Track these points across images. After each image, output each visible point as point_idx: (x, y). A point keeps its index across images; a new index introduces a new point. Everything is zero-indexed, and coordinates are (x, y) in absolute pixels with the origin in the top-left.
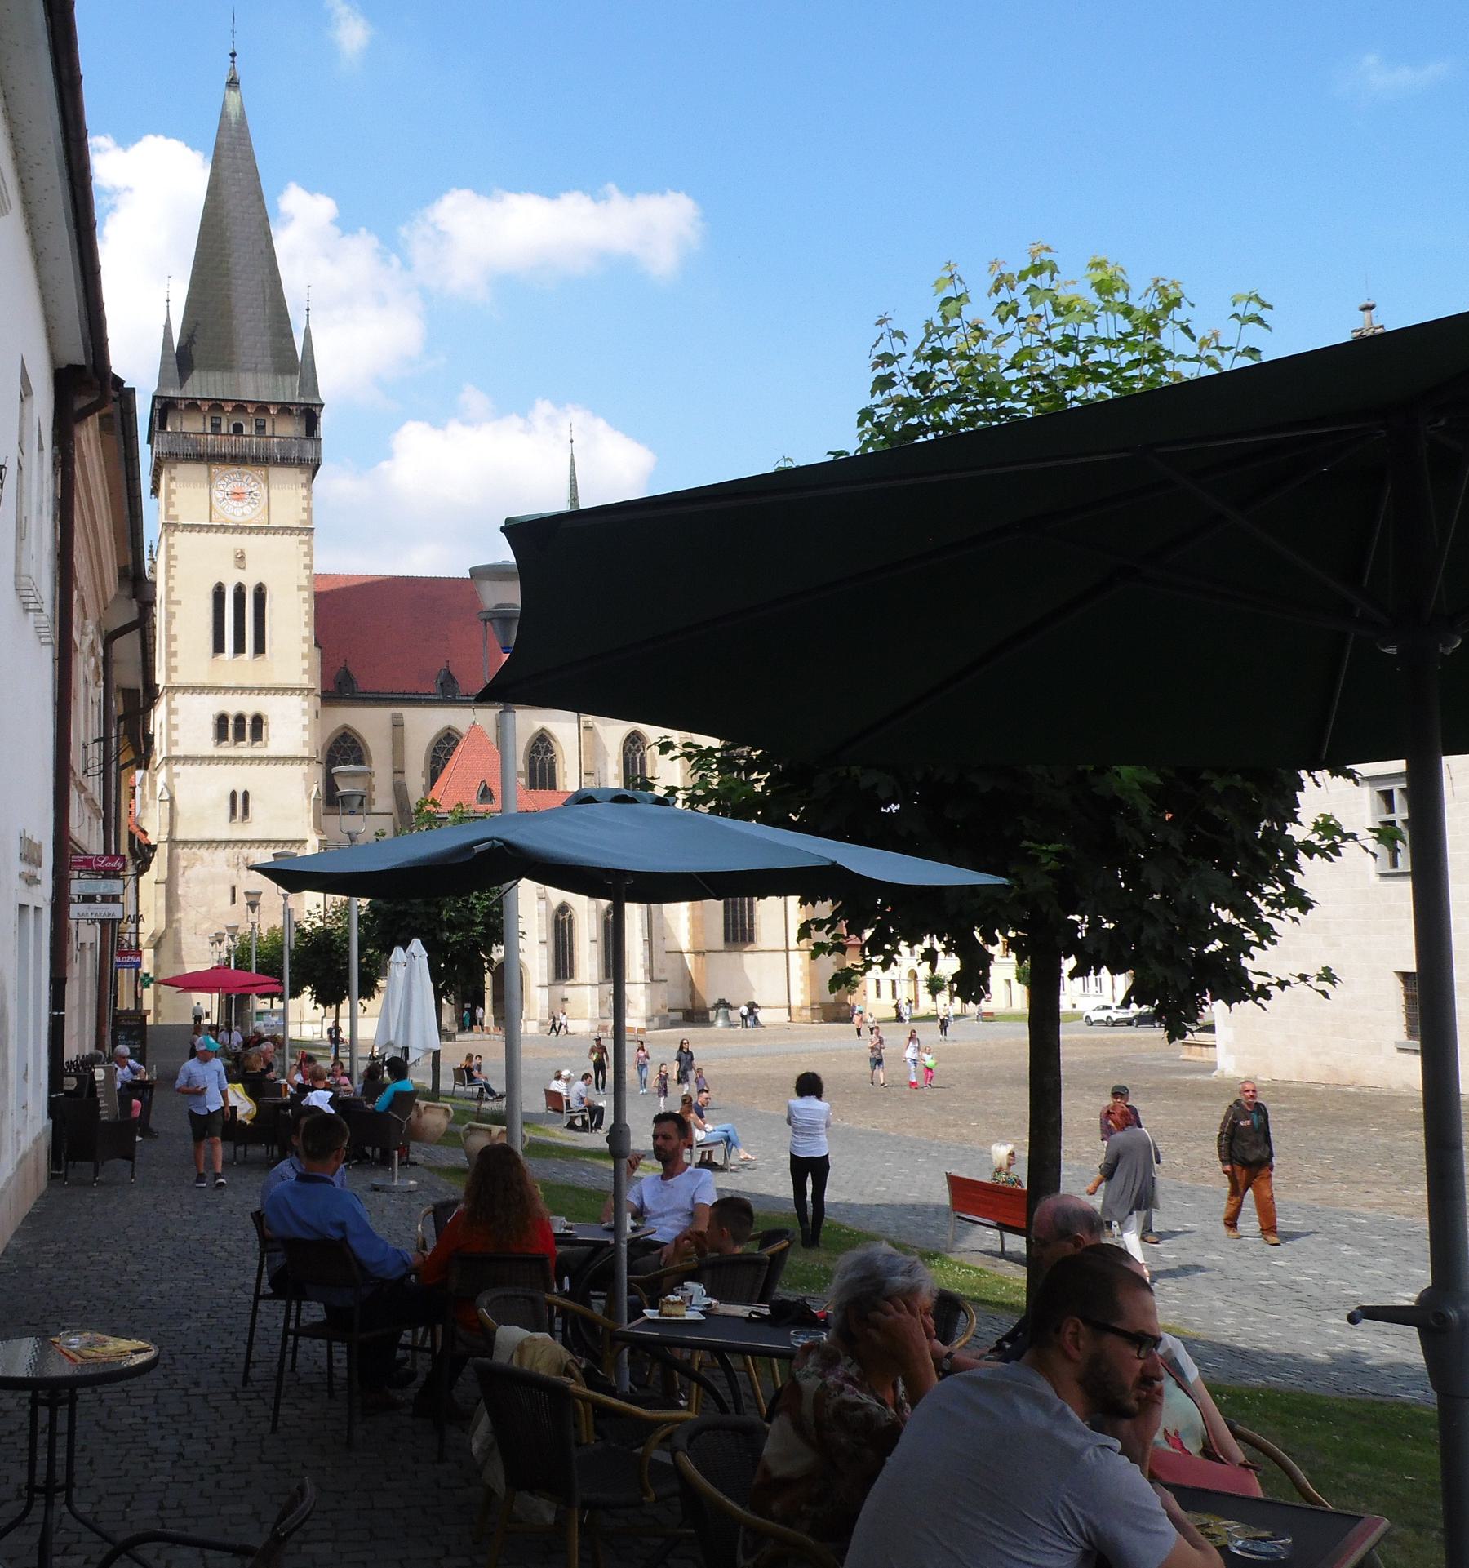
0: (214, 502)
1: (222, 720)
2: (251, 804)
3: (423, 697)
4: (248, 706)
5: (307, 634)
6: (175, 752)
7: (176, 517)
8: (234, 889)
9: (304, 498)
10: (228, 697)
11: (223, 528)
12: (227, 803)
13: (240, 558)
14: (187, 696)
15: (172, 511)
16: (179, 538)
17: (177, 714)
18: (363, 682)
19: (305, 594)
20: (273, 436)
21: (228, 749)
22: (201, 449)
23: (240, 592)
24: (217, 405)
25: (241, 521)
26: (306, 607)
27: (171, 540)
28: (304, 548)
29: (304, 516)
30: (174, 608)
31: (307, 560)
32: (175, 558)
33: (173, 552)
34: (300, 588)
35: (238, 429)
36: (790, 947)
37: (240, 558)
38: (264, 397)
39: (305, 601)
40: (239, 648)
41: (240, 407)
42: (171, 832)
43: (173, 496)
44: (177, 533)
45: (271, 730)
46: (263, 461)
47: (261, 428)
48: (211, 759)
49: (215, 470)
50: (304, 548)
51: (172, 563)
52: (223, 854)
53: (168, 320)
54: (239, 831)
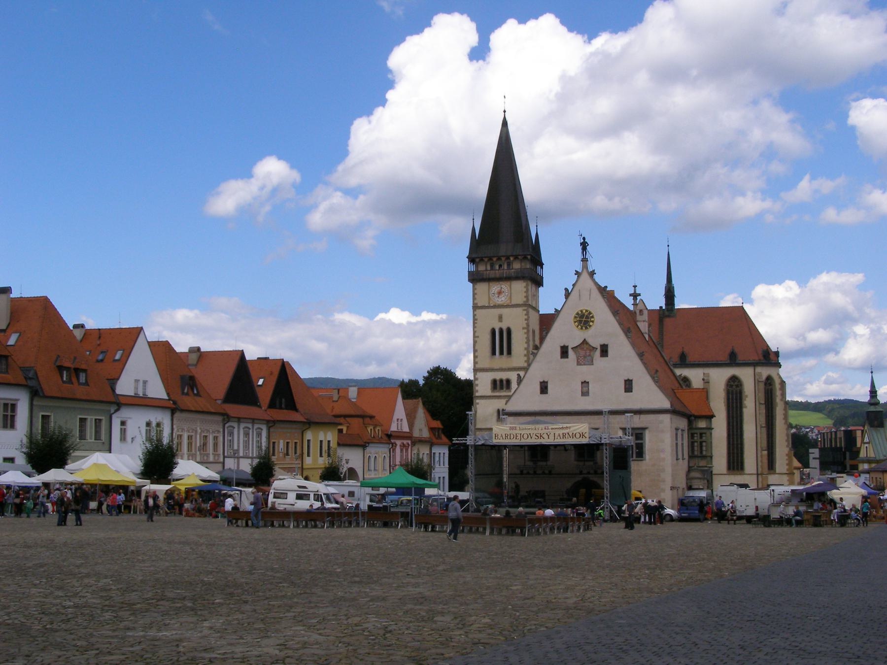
1: (494, 382)
4: (503, 376)
6: (477, 394)
7: (477, 304)
9: (525, 292)
11: (495, 307)
12: (496, 414)
13: (500, 318)
14: (481, 373)
15: (475, 302)
16: (478, 312)
19: (525, 331)
20: (512, 269)
22: (485, 277)
23: (501, 331)
27: (475, 313)
28: (525, 312)
29: (525, 299)
31: (526, 317)
32: (476, 320)
33: (476, 317)
34: (524, 328)
36: (759, 472)
37: (500, 318)
39: (525, 333)
46: (508, 279)
47: (509, 265)
49: (491, 284)
50: (525, 312)
53: (473, 227)
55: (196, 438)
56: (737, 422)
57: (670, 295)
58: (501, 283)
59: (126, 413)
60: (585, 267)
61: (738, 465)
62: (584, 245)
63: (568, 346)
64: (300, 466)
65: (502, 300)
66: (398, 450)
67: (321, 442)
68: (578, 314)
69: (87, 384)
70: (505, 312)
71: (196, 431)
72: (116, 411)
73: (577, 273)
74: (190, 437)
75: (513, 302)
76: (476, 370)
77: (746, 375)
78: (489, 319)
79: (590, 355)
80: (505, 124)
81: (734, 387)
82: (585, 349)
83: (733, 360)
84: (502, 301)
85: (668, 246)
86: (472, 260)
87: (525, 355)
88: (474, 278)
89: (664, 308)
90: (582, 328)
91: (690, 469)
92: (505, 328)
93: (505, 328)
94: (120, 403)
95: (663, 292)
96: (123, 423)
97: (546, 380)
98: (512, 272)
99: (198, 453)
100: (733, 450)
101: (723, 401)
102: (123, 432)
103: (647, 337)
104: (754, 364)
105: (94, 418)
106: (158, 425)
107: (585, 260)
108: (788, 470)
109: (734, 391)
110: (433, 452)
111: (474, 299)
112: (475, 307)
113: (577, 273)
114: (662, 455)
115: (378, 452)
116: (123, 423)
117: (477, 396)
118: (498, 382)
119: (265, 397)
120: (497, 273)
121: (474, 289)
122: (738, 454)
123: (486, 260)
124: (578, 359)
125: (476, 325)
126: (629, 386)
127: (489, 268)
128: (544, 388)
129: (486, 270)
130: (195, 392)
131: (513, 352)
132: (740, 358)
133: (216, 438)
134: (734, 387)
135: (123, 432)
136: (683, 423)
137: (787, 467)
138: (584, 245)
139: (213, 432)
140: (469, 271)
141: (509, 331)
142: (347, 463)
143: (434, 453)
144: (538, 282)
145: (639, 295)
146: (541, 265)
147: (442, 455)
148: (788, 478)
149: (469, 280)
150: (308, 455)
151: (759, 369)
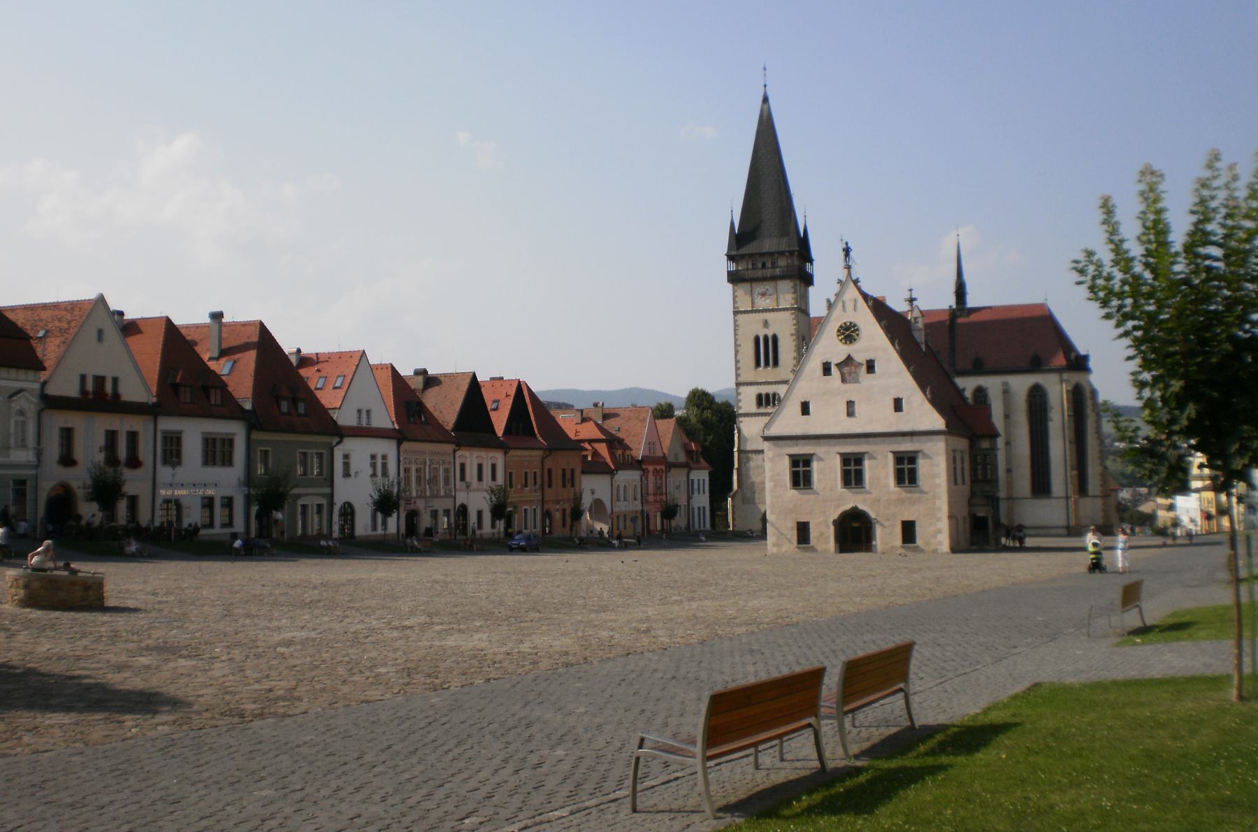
1: (759, 397)
6: (740, 412)
7: (738, 308)
10: (763, 386)
11: (759, 311)
13: (766, 324)
15: (736, 305)
16: (740, 317)
19: (794, 337)
20: (777, 267)
21: (762, 410)
22: (746, 277)
23: (766, 338)
24: (751, 256)
28: (793, 316)
30: (739, 348)
32: (738, 326)
33: (737, 323)
34: (792, 335)
35: (764, 265)
37: (766, 324)
38: (773, 250)
41: (762, 255)
42: (739, 448)
46: (774, 278)
47: (773, 263)
50: (793, 316)
55: (425, 468)
58: (765, 283)
59: (350, 445)
60: (849, 274)
62: (847, 251)
63: (830, 363)
64: (540, 498)
66: (651, 477)
67: (564, 470)
68: (841, 327)
69: (306, 415)
70: (770, 316)
71: (425, 463)
72: (338, 443)
73: (840, 282)
74: (418, 470)
76: (738, 384)
78: (754, 326)
80: (766, 100)
83: (1036, 365)
86: (731, 258)
88: (734, 278)
89: (954, 307)
90: (846, 343)
91: (973, 494)
92: (770, 335)
93: (770, 335)
94: (342, 433)
96: (346, 457)
97: (807, 400)
98: (778, 271)
99: (427, 486)
102: (347, 466)
103: (923, 347)
105: (315, 451)
106: (384, 457)
107: (848, 267)
110: (691, 478)
111: (735, 302)
112: (736, 313)
113: (840, 282)
114: (937, 481)
115: (630, 478)
116: (346, 457)
119: (499, 421)
120: (759, 273)
121: (734, 291)
125: (737, 332)
126: (898, 405)
127: (750, 266)
128: (805, 409)
129: (748, 269)
130: (423, 419)
133: (447, 470)
135: (347, 466)
136: (962, 444)
138: (847, 251)
139: (444, 463)
140: (728, 271)
141: (775, 338)
142: (593, 493)
143: (693, 480)
144: (808, 280)
145: (915, 299)
146: (811, 261)
147: (701, 482)
149: (729, 281)
150: (550, 486)
151: (1065, 376)
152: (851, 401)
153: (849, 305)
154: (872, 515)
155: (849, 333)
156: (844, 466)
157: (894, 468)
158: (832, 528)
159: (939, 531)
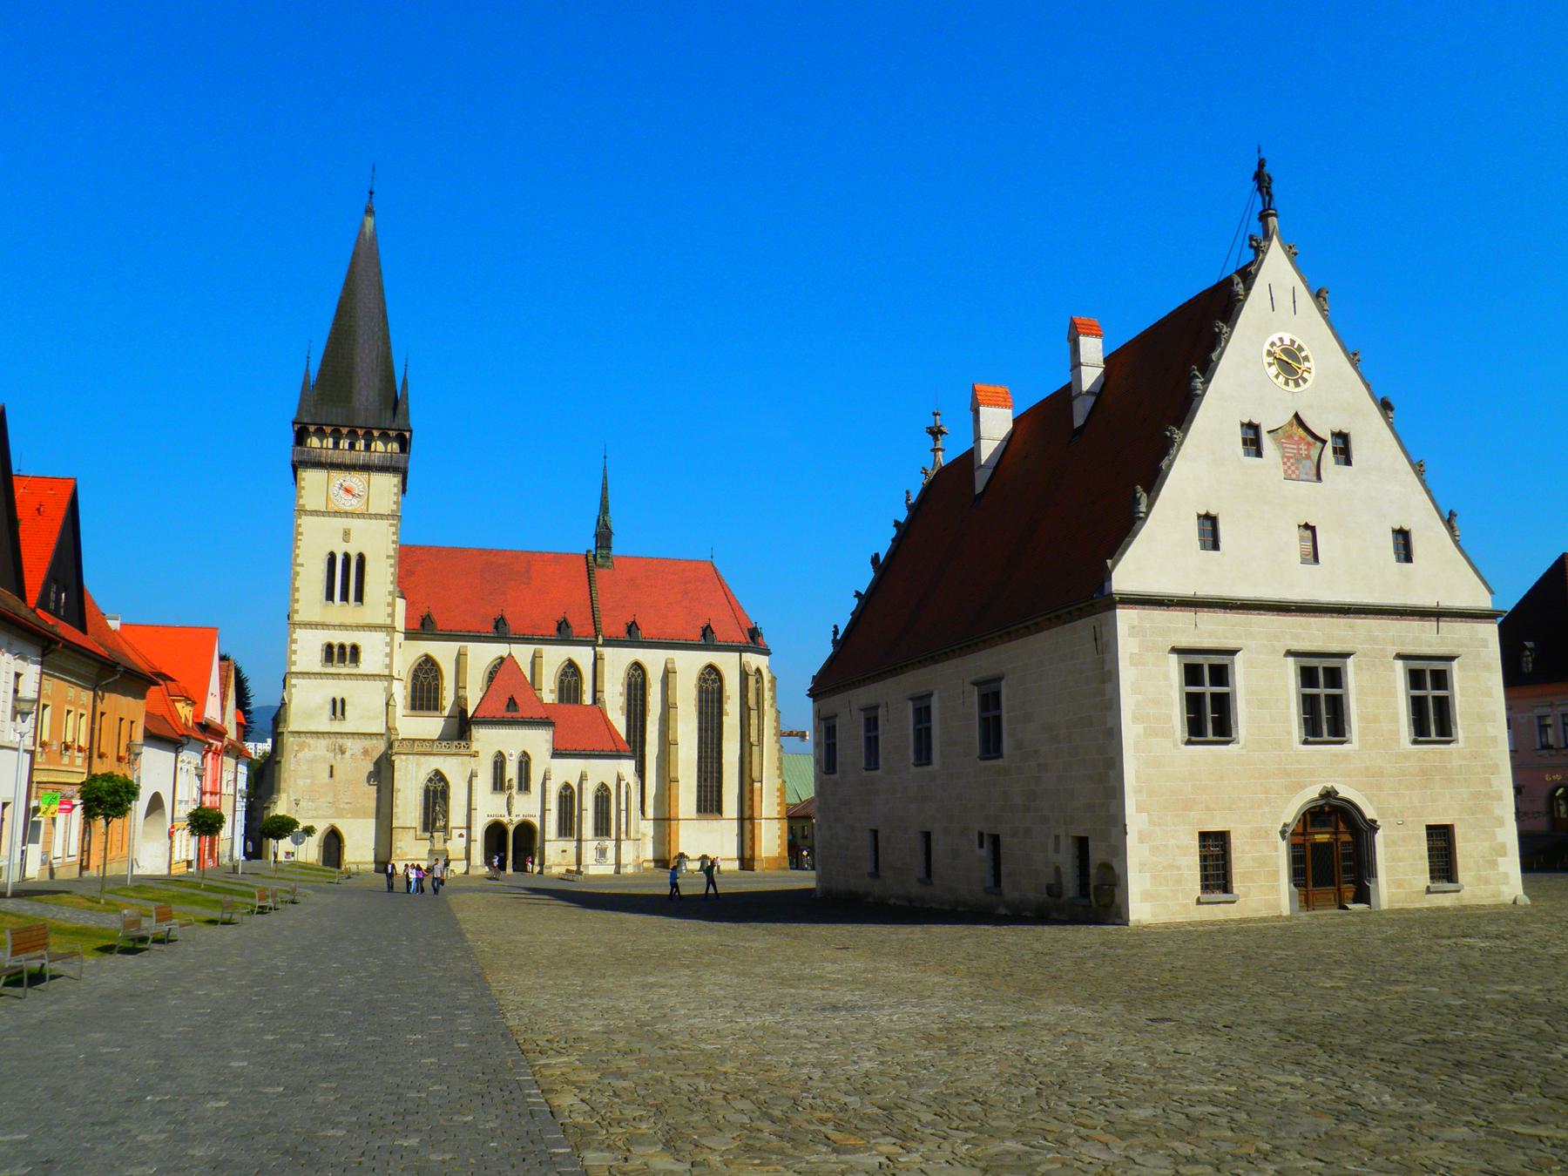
0: (331, 495)
1: (329, 647)
2: (346, 708)
3: (483, 635)
4: (347, 638)
5: (392, 590)
6: (294, 669)
7: (304, 506)
8: (332, 767)
11: (337, 514)
12: (329, 707)
13: (346, 535)
15: (301, 502)
17: (296, 643)
18: (441, 622)
19: (392, 561)
22: (323, 460)
23: (347, 557)
25: (349, 509)
26: (392, 570)
27: (299, 521)
28: (393, 529)
29: (394, 507)
32: (301, 534)
34: (388, 557)
35: (352, 446)
37: (346, 535)
39: (391, 566)
40: (345, 597)
43: (303, 491)
44: (303, 517)
45: (363, 656)
46: (367, 468)
47: (368, 447)
48: (320, 674)
50: (393, 529)
51: (299, 537)
52: (324, 743)
53: (307, 370)
54: (337, 727)
56: (712, 739)
57: (604, 537)
61: (712, 805)
62: (1262, 180)
65: (349, 503)
75: (372, 511)
77: (728, 663)
79: (1308, 457)
81: (710, 682)
82: (1296, 438)
83: (707, 640)
84: (351, 505)
85: (605, 457)
87: (389, 605)
95: (591, 529)
98: (375, 458)
100: (706, 780)
101: (694, 702)
104: (741, 650)
108: (779, 812)
109: (710, 688)
117: (293, 673)
118: (336, 650)
120: (349, 457)
122: (712, 787)
123: (328, 430)
124: (1285, 463)
125: (299, 543)
126: (1403, 544)
127: (331, 446)
131: (366, 598)
132: (720, 636)
134: (710, 682)
137: (779, 808)
138: (1262, 180)
141: (361, 559)
148: (779, 826)
151: (747, 657)
152: (1306, 526)
153: (1283, 299)
154: (1370, 813)
155: (1289, 362)
156: (1304, 686)
157: (1407, 695)
158: (1283, 848)
159: (1501, 851)
